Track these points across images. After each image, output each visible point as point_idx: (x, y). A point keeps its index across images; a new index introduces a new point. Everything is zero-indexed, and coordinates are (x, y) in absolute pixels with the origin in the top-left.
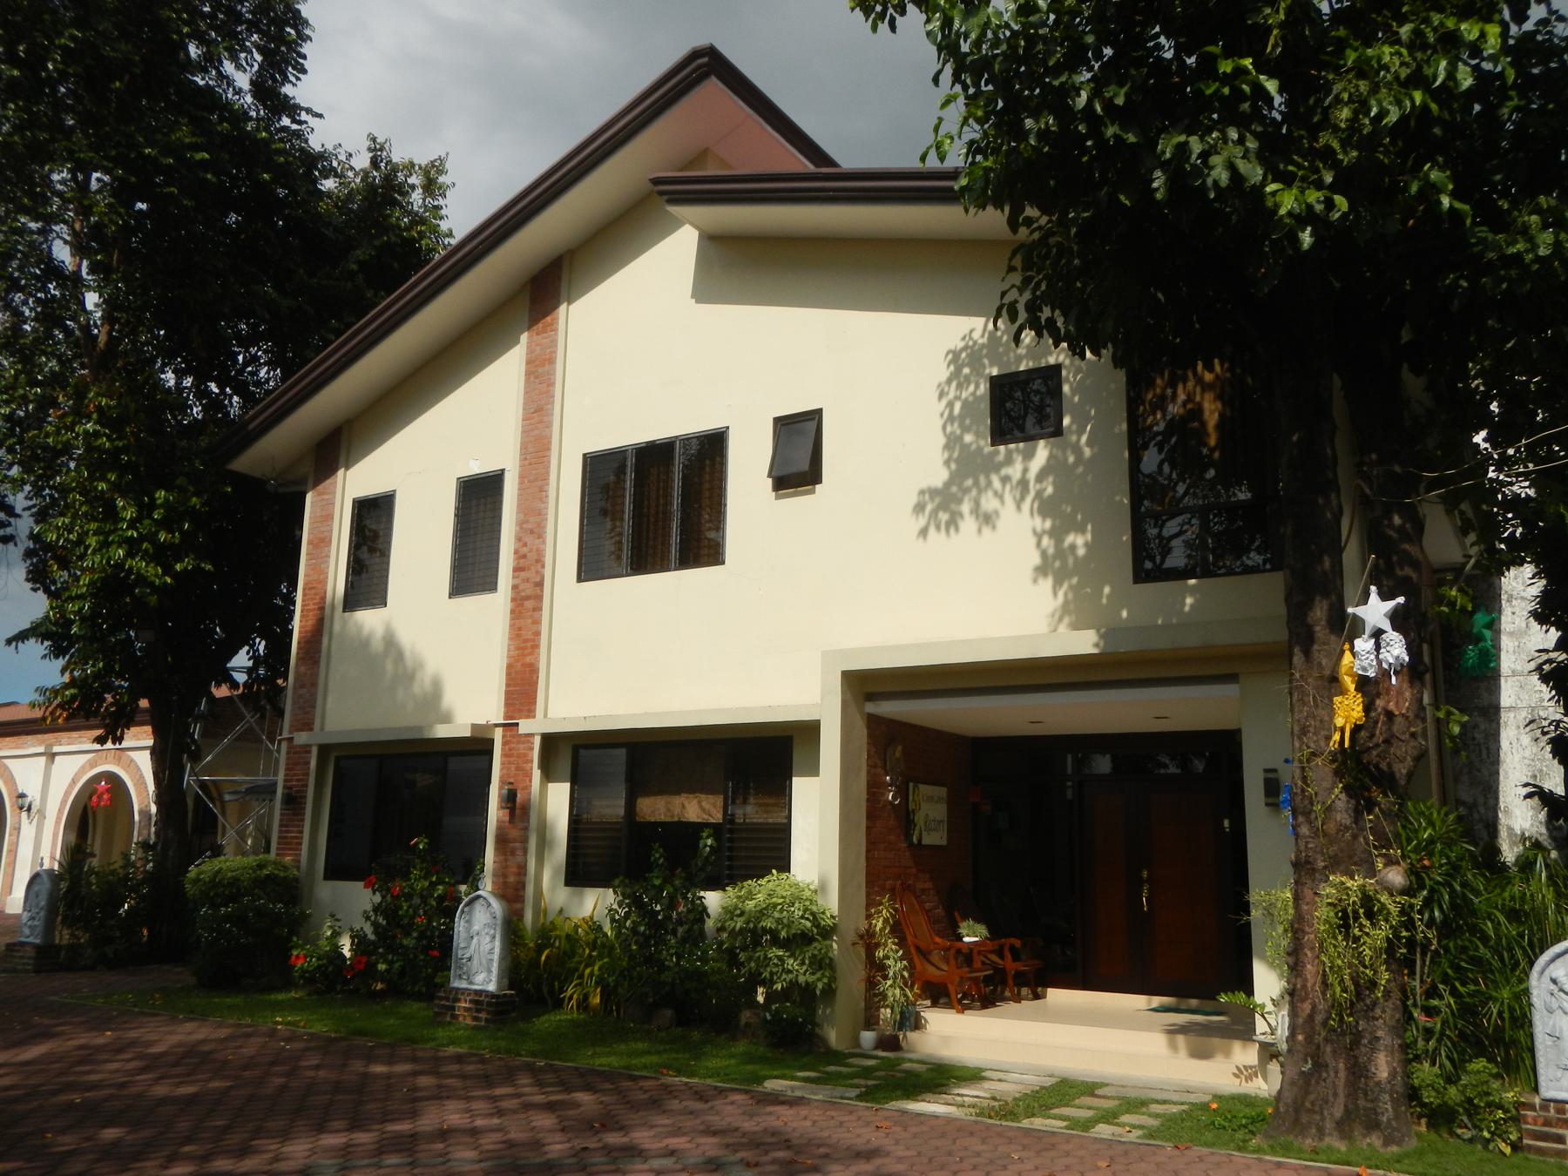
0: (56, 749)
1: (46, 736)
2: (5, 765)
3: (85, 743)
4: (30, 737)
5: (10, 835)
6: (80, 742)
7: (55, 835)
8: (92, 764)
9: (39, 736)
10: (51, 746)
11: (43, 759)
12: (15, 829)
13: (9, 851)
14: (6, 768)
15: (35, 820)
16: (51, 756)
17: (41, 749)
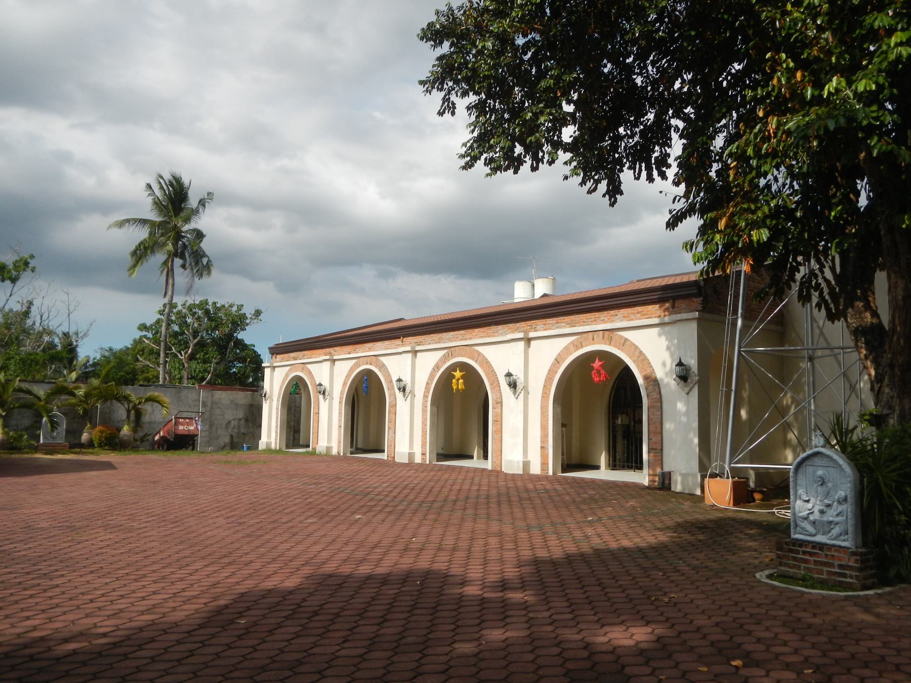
0: (532, 334)
1: (518, 324)
2: (478, 351)
3: (564, 327)
4: (500, 327)
5: (494, 408)
6: (558, 327)
7: (544, 409)
8: (577, 346)
9: (510, 325)
10: (526, 332)
11: (521, 344)
12: (497, 403)
13: (495, 421)
14: (480, 354)
15: (522, 395)
16: (528, 341)
17: (521, 335)
